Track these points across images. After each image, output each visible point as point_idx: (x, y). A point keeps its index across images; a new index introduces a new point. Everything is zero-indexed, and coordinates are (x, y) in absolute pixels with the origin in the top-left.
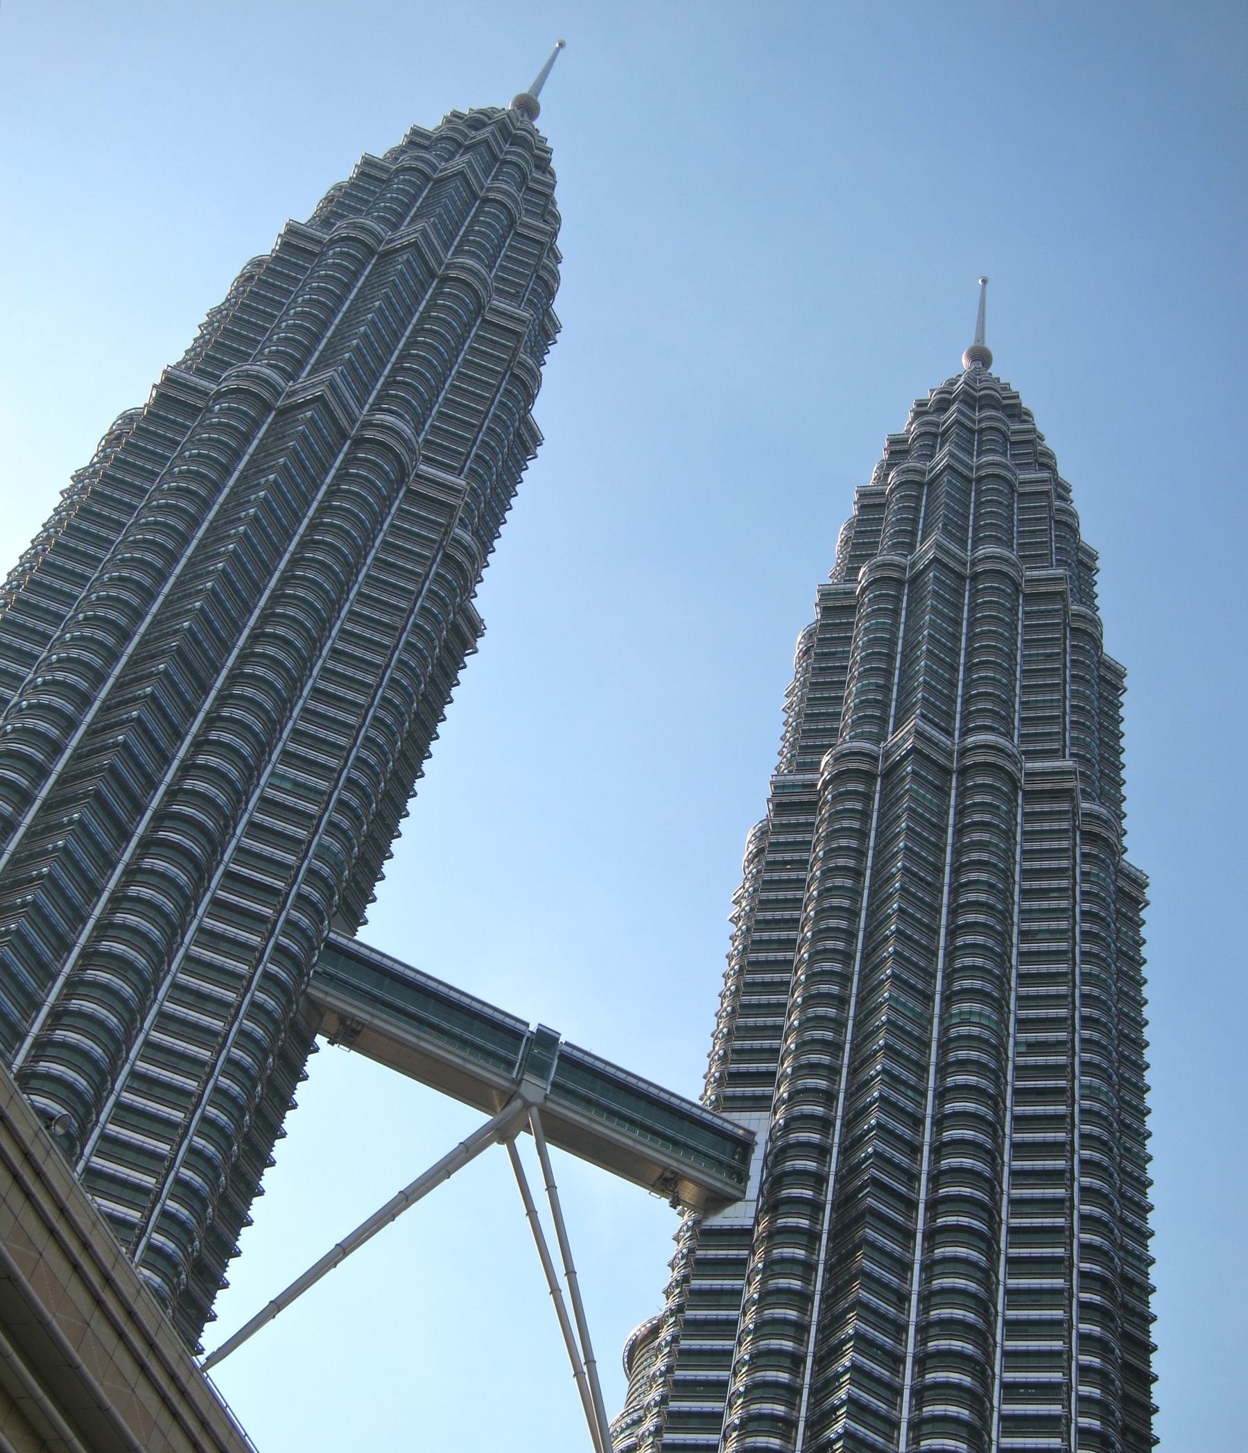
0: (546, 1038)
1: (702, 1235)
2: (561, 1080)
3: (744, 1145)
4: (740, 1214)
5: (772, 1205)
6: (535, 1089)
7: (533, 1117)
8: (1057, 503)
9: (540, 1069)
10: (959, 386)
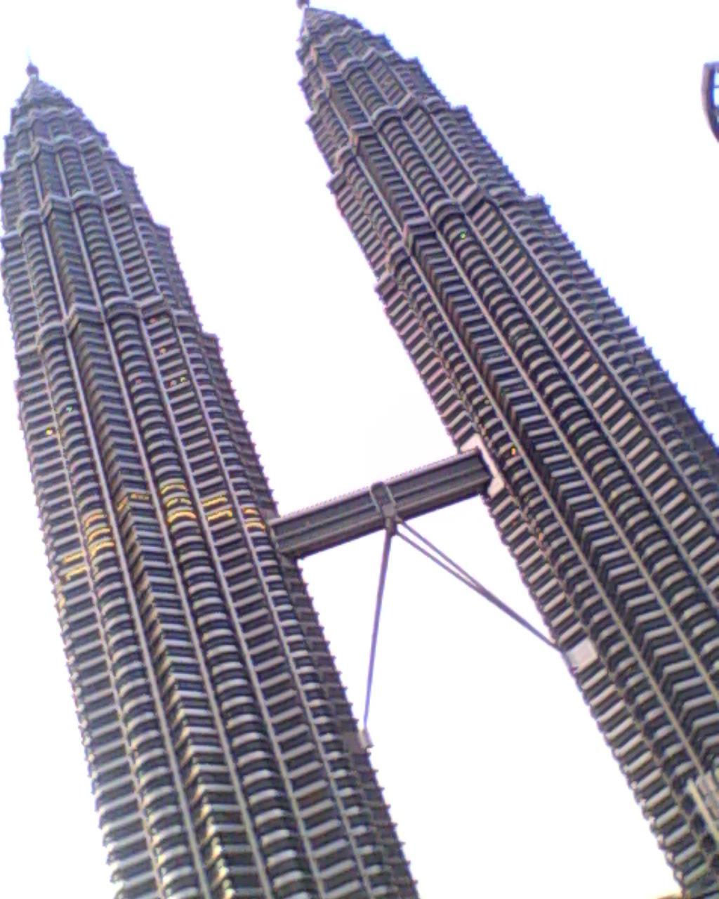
0: (378, 487)
1: (492, 503)
2: (396, 495)
3: (477, 455)
4: (497, 485)
5: (507, 474)
6: (390, 511)
7: (398, 519)
8: (387, 53)
9: (383, 500)
10: (306, 33)
